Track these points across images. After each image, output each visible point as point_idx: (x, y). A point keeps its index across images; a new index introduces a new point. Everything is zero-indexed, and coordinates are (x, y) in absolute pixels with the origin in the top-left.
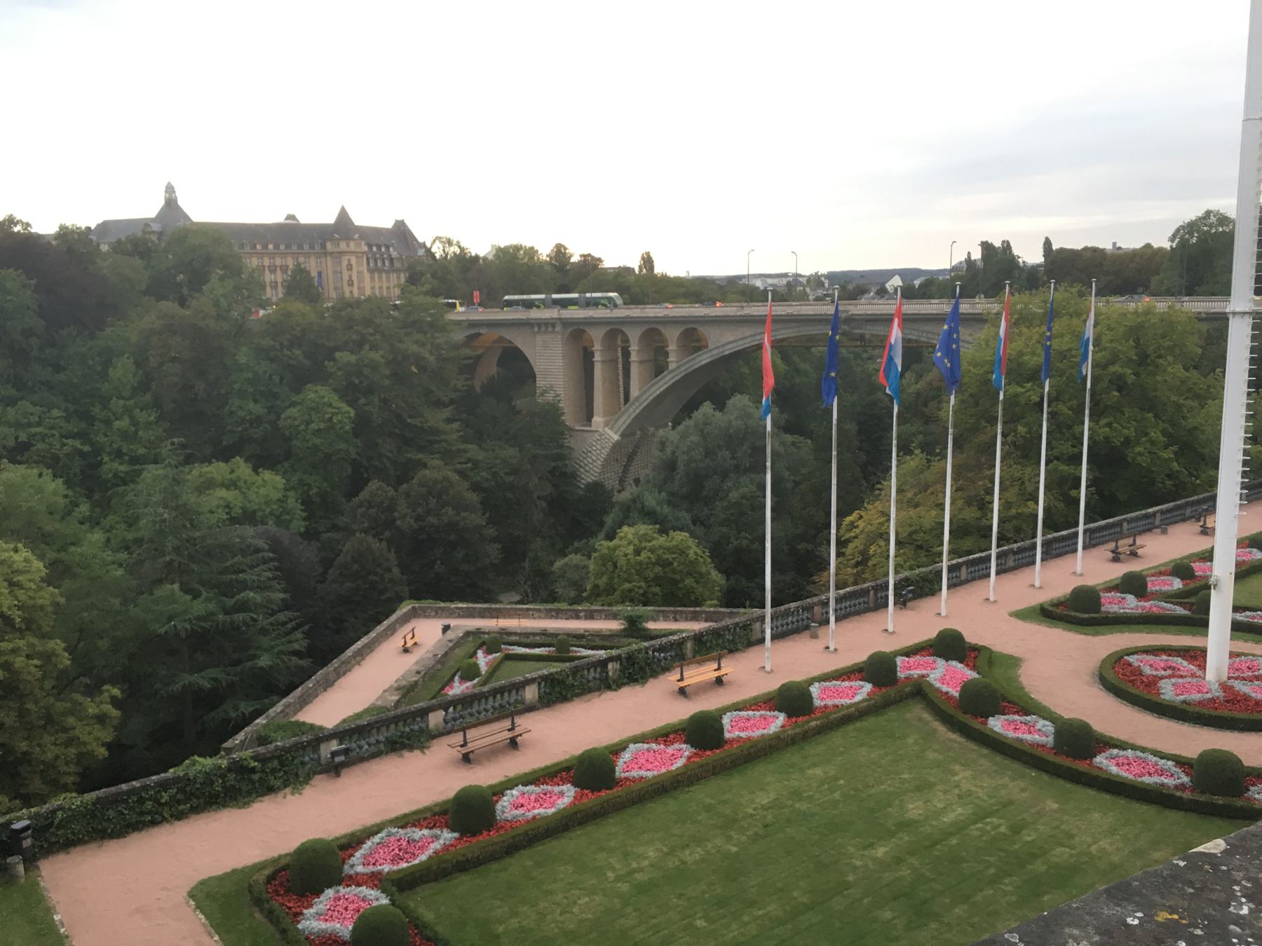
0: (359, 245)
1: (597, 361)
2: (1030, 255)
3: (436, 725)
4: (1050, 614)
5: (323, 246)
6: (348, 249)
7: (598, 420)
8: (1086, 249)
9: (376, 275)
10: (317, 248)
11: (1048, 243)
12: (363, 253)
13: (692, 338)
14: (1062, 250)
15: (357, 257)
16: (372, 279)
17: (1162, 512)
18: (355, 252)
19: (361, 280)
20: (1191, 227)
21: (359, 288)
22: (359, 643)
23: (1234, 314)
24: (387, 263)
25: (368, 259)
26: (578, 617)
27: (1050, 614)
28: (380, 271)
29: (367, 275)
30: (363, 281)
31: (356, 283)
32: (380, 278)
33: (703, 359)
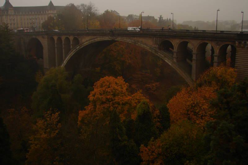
13: (77, 42)
18: (53, 13)
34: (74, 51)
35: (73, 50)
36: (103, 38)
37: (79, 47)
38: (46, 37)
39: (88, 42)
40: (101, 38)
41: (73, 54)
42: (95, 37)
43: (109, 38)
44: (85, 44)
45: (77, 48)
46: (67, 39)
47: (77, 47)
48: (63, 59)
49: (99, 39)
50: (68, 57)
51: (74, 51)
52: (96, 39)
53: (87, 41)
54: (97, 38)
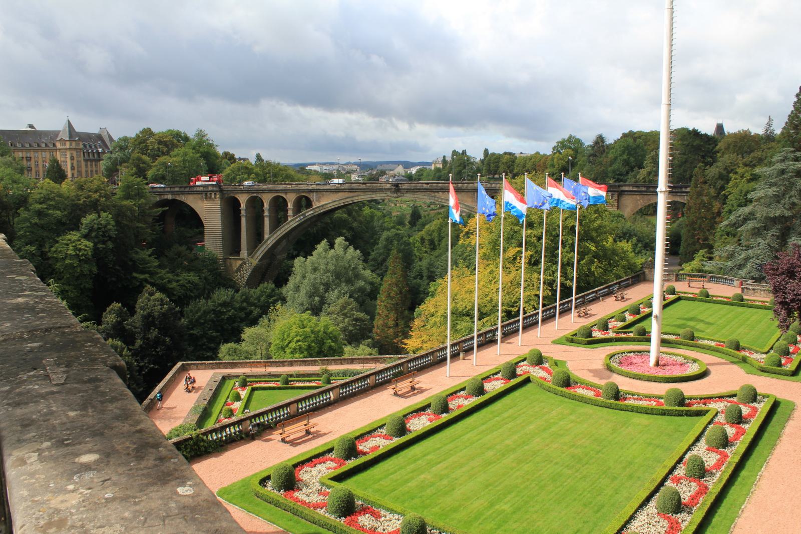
0: (78, 144)
1: (266, 216)
2: (477, 155)
3: (294, 412)
4: (571, 340)
5: (54, 145)
6: (71, 147)
7: (244, 253)
8: (505, 153)
9: (89, 163)
10: (51, 146)
11: (486, 151)
12: (80, 149)
13: (304, 202)
14: (493, 154)
15: (77, 152)
16: (86, 166)
17: (600, 290)
19: (79, 166)
20: (562, 144)
21: (78, 171)
22: (160, 385)
23: (661, 192)
24: (96, 156)
25: (84, 153)
26: (284, 366)
27: (571, 340)
28: (91, 161)
29: (83, 163)
30: (81, 167)
31: (76, 168)
32: (91, 165)
33: (309, 213)
34: (298, 219)
35: (296, 218)
36: (374, 196)
37: (312, 212)
38: (218, 196)
39: (337, 203)
40: (369, 196)
41: (295, 225)
42: (356, 194)
43: (388, 196)
44: (327, 206)
45: (307, 214)
46: (255, 203)
47: (308, 212)
48: (266, 236)
49: (362, 197)
50: (279, 233)
51: (298, 219)
52: (357, 198)
53: (335, 201)
54: (358, 196)
